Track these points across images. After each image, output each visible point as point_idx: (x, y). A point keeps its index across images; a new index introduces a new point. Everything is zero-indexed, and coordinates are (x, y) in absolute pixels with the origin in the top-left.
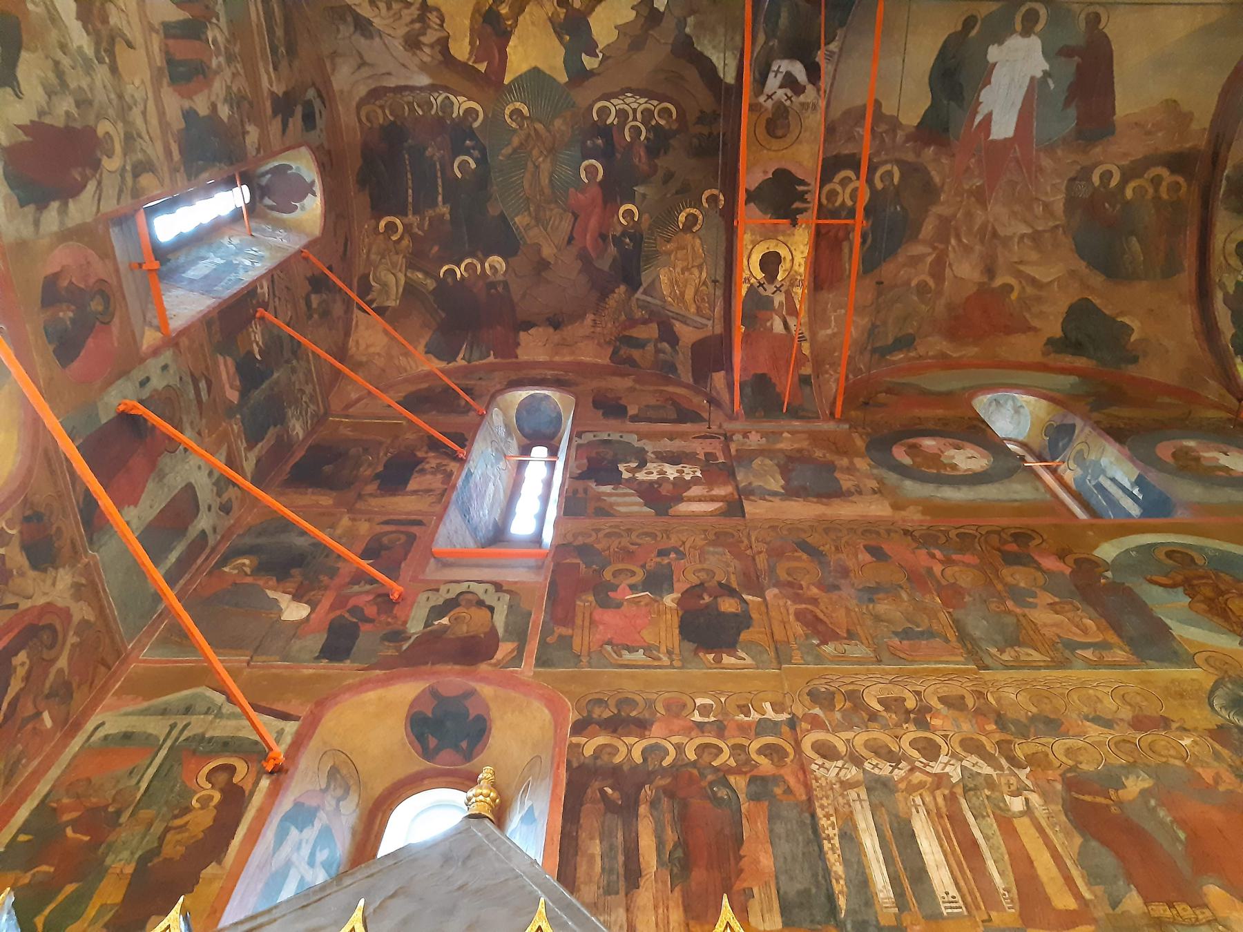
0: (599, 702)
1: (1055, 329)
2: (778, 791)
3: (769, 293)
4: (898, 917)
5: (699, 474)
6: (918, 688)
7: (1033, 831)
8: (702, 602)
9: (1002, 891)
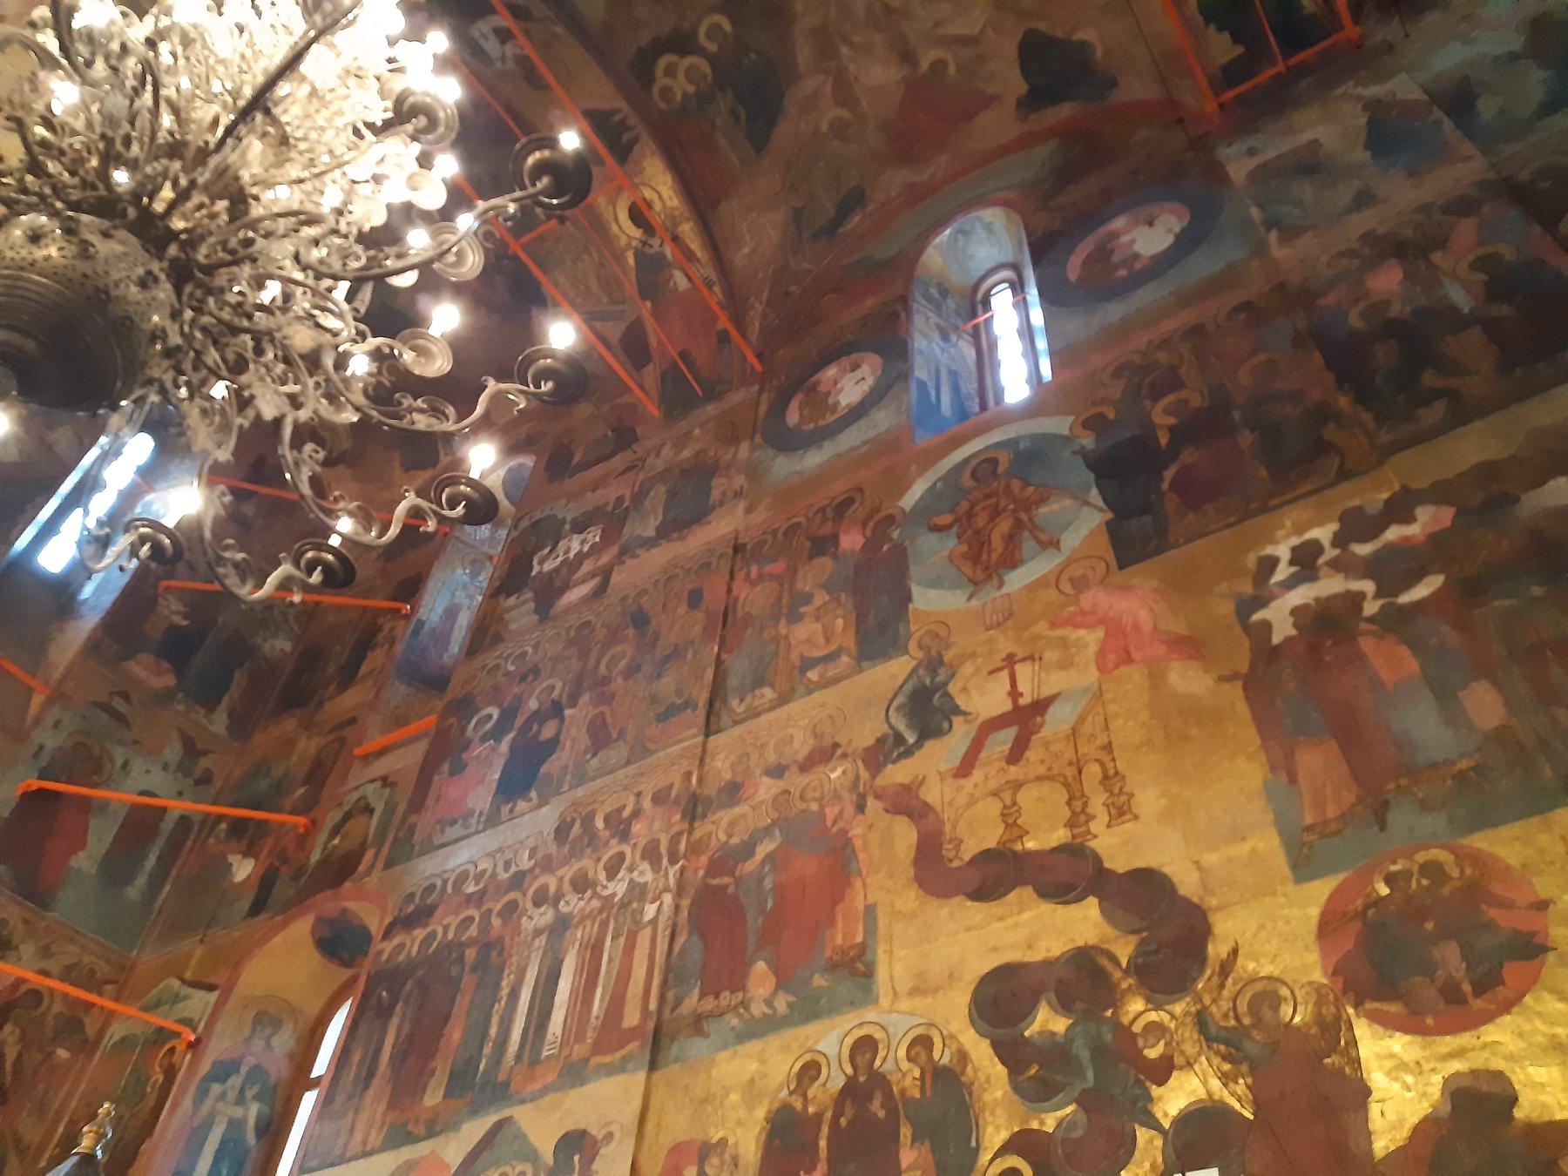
0: (412, 895)
1: (1014, 84)
2: (494, 954)
3: (656, 248)
4: (512, 1068)
5: (597, 539)
6: (642, 787)
7: (647, 944)
8: (531, 734)
9: (593, 1020)
